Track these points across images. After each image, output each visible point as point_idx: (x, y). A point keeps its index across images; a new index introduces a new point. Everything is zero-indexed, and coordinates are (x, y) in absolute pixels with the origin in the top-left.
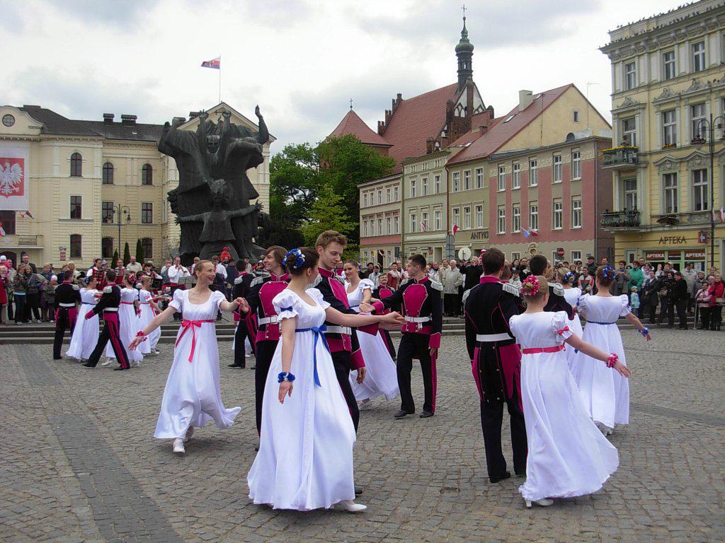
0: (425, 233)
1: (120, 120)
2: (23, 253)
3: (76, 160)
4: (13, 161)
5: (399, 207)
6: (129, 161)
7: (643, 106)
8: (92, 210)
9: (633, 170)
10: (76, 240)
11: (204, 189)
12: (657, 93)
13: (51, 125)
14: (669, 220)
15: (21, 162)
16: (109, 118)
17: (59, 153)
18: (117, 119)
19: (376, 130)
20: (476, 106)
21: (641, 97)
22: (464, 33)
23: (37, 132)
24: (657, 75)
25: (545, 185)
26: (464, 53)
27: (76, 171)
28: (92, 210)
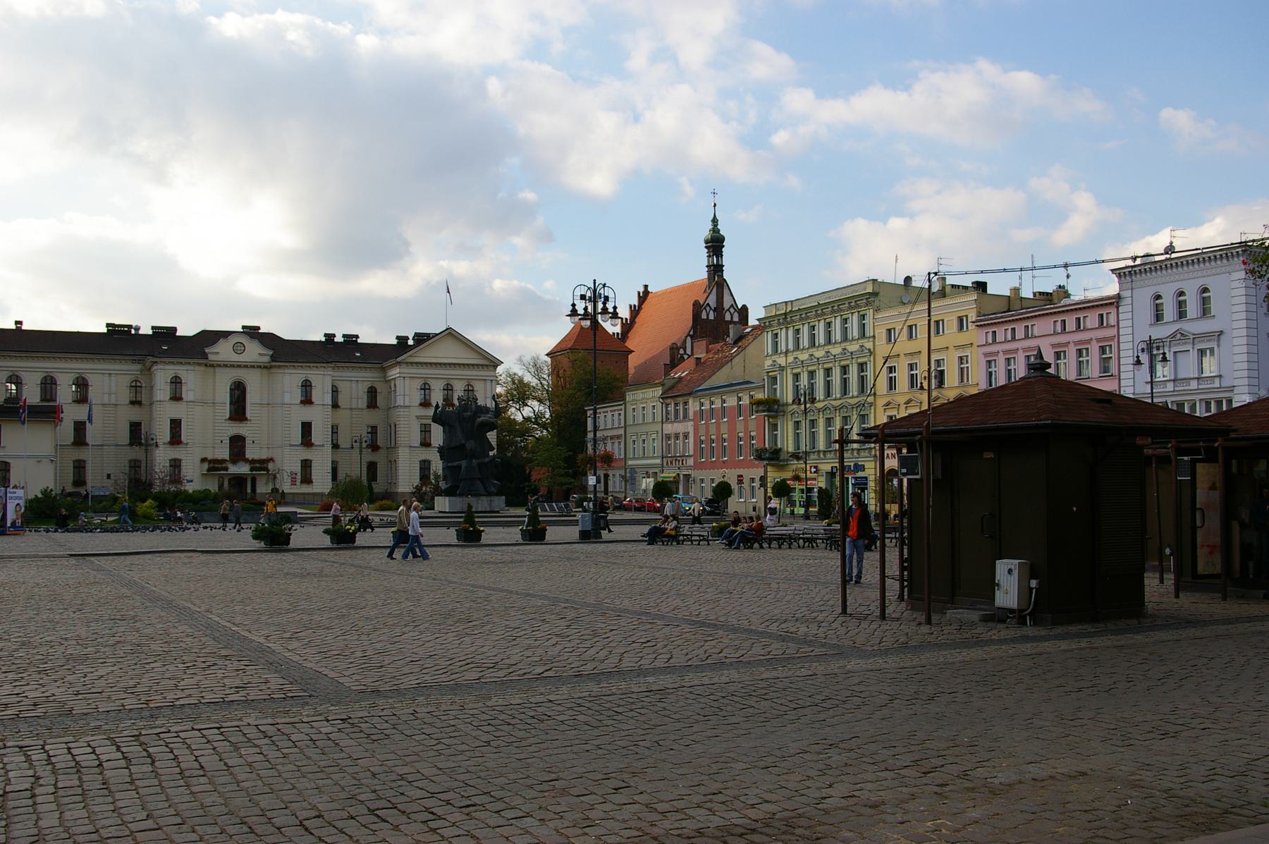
0: (644, 458)
1: (341, 340)
3: (307, 386)
5: (621, 432)
6: (354, 384)
7: (782, 369)
9: (775, 417)
10: (306, 465)
11: (462, 447)
12: (790, 359)
13: (284, 352)
14: (796, 456)
16: (330, 337)
17: (290, 380)
20: (726, 305)
21: (781, 361)
22: (715, 221)
23: (267, 359)
24: (791, 347)
25: (732, 424)
26: (715, 244)
28: (320, 435)
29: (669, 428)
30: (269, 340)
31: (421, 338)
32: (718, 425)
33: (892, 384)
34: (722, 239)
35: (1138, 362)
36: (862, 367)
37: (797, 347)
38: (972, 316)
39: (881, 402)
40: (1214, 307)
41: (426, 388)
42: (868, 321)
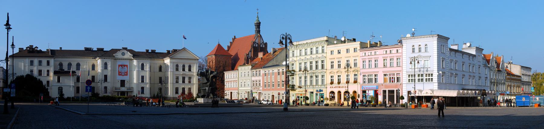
2: (127, 92)
3: (143, 65)
4: (125, 66)
5: (237, 79)
8: (147, 80)
10: (143, 88)
12: (298, 58)
15: (127, 66)
16: (147, 51)
18: (150, 51)
19: (226, 49)
21: (295, 59)
22: (258, 17)
24: (298, 55)
26: (258, 25)
27: (143, 68)
29: (254, 78)
30: (131, 51)
31: (175, 51)
32: (271, 77)
33: (332, 66)
34: (260, 23)
35: (411, 63)
36: (322, 61)
37: (300, 55)
38: (359, 48)
39: (328, 72)
40: (429, 49)
41: (177, 66)
42: (325, 48)
